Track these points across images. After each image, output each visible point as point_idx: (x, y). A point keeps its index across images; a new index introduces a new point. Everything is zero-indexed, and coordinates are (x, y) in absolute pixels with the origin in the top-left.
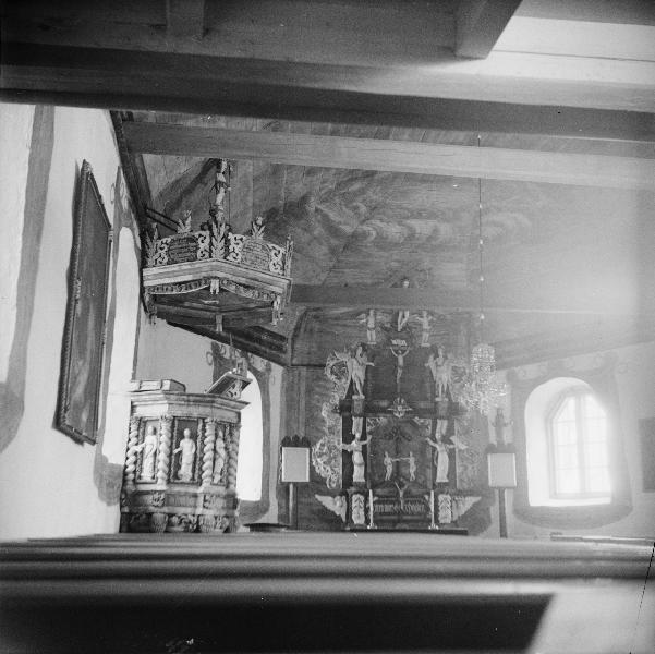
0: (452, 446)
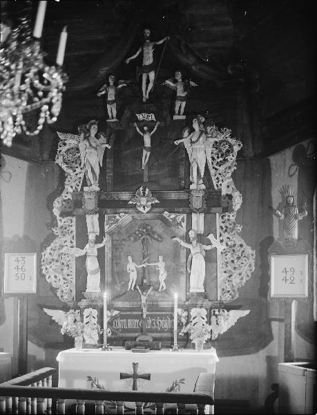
0: (209, 248)
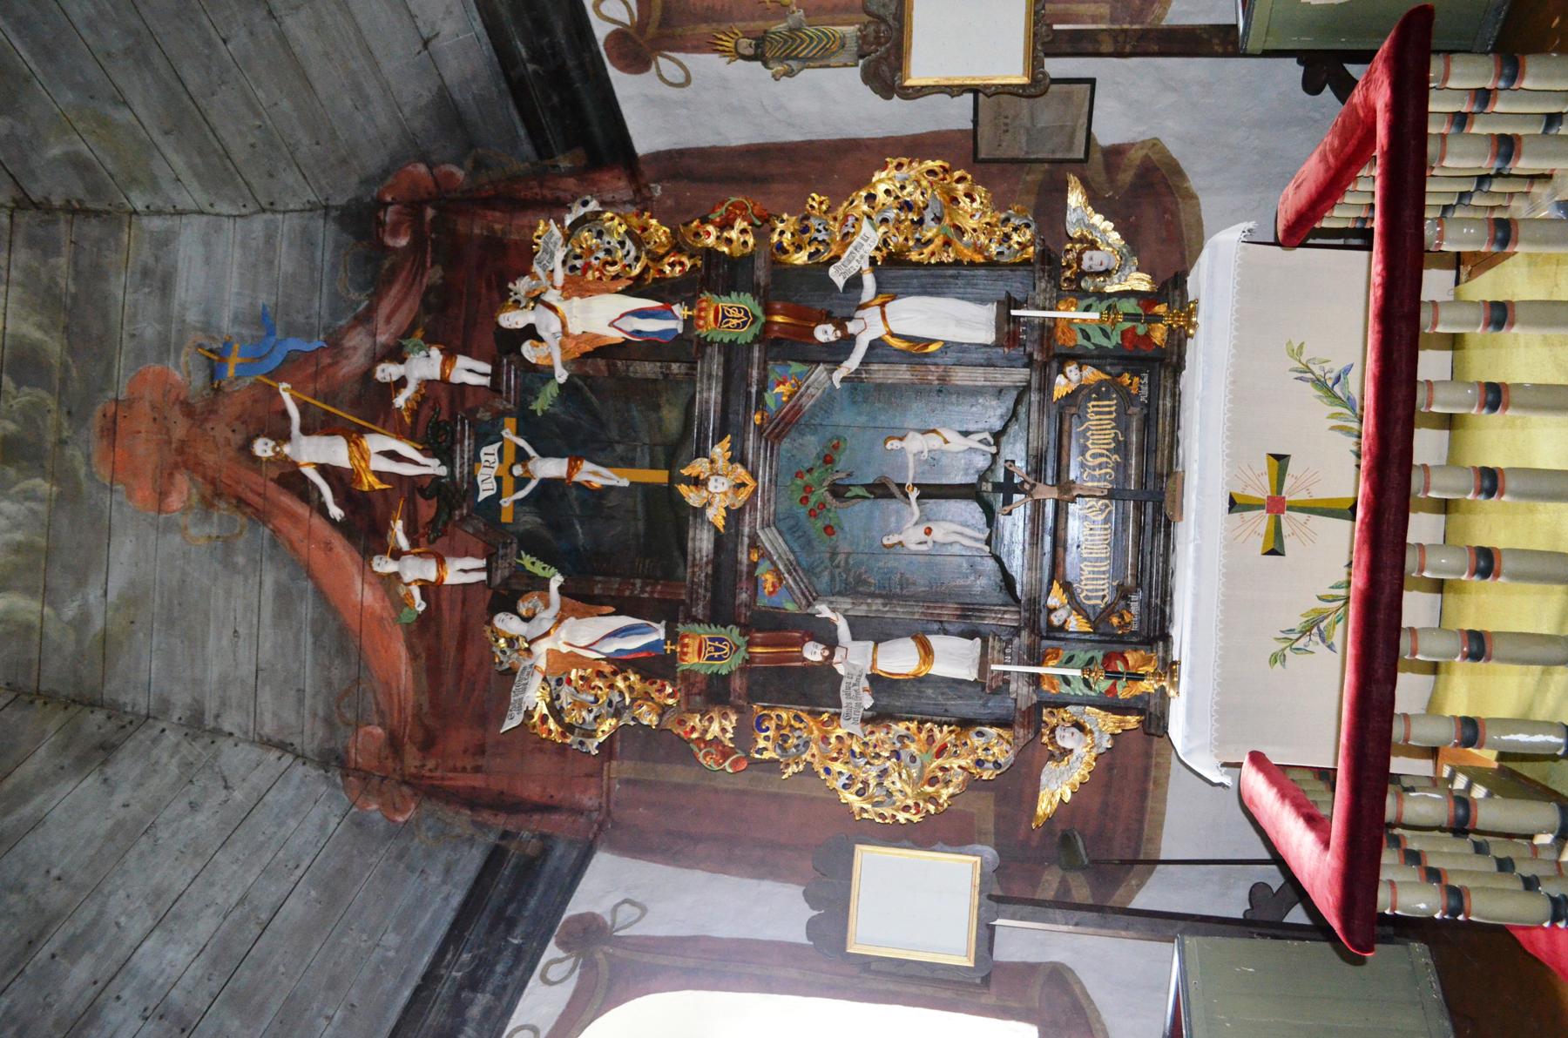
0: (869, 280)
